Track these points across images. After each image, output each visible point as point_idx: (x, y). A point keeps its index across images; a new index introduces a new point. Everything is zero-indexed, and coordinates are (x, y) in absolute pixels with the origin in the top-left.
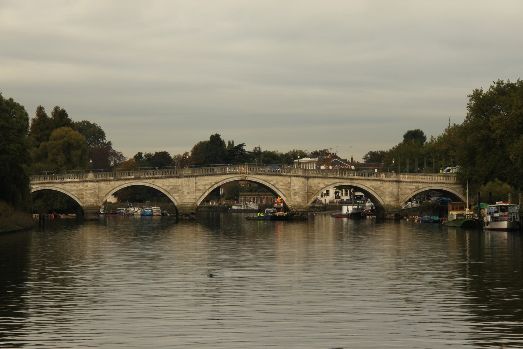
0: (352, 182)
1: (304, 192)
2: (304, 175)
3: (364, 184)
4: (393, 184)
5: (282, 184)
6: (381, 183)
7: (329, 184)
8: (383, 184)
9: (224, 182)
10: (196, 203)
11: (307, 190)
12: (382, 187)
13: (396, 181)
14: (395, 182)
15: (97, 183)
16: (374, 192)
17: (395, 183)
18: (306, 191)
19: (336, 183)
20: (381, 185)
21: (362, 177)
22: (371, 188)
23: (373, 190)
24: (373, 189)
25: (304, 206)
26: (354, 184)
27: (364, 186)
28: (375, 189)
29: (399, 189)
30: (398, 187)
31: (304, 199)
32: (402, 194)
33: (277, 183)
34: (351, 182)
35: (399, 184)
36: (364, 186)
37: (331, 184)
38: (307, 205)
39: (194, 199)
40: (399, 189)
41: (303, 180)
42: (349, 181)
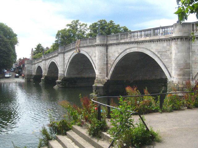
0: (139, 46)
1: (103, 64)
2: (102, 43)
3: (150, 48)
4: (177, 44)
5: (94, 55)
6: (167, 45)
7: (121, 52)
8: (170, 46)
9: (73, 56)
10: (64, 75)
11: (107, 61)
12: (169, 50)
13: (181, 38)
14: (179, 40)
15: (45, 61)
16: (160, 59)
17: (179, 42)
18: (105, 61)
19: (126, 50)
20: (168, 47)
21: (148, 38)
22: (156, 53)
23: (159, 57)
24: (159, 56)
25: (102, 80)
26: (141, 50)
27: (149, 50)
28: (161, 55)
29: (191, 53)
30: (189, 48)
31: (102, 72)
32: (196, 63)
33: (92, 55)
34: (138, 47)
35: (189, 44)
36: (149, 50)
37: (123, 51)
38: (106, 78)
39: (62, 71)
40: (191, 53)
41: (103, 49)
42: (135, 45)
